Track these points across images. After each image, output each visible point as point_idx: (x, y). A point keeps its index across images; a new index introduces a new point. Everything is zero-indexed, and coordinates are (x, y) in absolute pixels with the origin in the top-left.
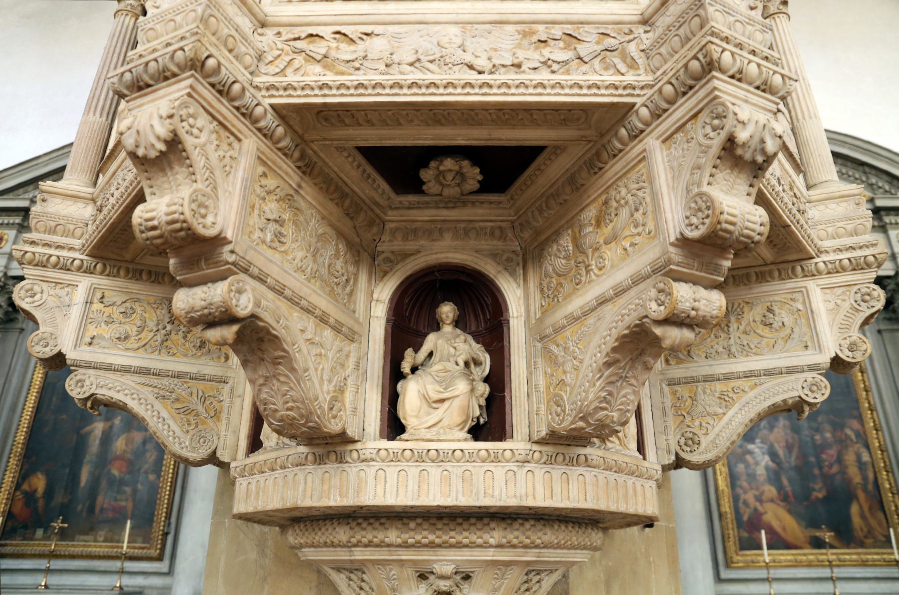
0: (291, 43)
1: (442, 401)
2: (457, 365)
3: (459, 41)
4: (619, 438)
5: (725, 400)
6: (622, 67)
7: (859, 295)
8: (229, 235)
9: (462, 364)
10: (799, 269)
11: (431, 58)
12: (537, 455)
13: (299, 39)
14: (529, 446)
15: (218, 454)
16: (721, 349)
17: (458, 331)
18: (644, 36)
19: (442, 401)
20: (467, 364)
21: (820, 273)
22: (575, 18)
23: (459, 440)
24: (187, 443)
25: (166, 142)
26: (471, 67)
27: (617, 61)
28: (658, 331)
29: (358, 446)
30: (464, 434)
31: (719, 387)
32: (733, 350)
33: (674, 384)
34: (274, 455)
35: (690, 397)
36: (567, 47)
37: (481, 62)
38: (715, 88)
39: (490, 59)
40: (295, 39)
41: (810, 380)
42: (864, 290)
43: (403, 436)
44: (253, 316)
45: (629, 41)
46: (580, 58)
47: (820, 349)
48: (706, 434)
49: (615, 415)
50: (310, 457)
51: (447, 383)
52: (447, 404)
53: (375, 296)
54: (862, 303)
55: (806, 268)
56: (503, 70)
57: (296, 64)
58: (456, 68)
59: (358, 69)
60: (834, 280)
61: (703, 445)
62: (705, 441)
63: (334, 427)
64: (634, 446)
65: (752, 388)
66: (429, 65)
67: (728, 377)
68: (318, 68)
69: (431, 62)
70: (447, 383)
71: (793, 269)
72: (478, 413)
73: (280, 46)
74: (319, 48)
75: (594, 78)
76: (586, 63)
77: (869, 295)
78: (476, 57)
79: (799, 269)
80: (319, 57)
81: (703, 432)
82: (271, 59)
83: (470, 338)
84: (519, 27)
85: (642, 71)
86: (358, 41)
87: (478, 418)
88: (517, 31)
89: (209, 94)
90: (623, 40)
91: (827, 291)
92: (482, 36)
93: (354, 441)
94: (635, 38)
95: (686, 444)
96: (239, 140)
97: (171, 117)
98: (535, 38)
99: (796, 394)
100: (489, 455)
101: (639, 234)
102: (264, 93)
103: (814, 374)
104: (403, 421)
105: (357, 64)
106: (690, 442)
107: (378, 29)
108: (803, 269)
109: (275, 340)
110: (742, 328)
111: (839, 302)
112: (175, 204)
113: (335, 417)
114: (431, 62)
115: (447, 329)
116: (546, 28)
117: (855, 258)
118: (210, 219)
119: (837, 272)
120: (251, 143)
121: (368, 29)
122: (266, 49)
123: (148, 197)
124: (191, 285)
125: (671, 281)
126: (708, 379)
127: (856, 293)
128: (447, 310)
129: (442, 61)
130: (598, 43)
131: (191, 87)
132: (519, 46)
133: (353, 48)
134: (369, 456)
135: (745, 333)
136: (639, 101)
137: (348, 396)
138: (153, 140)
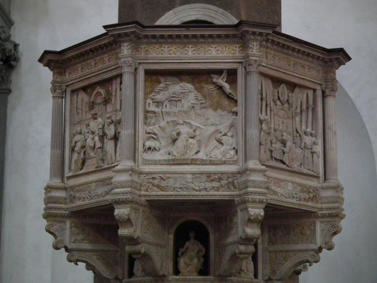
0: (148, 180)
1: (190, 264)
2: (195, 253)
3: (191, 180)
4: (245, 273)
5: (285, 259)
6: (232, 188)
7: (331, 225)
8: (140, 236)
9: (196, 253)
10: (313, 215)
11: (184, 186)
12: (216, 280)
13: (150, 178)
14: (214, 277)
15: (119, 276)
16: (286, 241)
17: (195, 241)
18: (239, 178)
19: (190, 264)
20: (198, 252)
21: (319, 217)
22: (221, 172)
23: (195, 276)
24: (108, 274)
25: (127, 219)
26: (194, 190)
27: (231, 186)
28: (238, 255)
29: (167, 277)
30: (196, 274)
31: (284, 254)
32: (290, 242)
33: (270, 252)
34: (141, 279)
35: (275, 257)
36: (219, 181)
37: (197, 188)
38: (247, 206)
39: (199, 187)
40: (149, 179)
41: (311, 254)
42: (333, 224)
43: (180, 275)
44: (145, 252)
45: (235, 179)
46: (221, 185)
47: (315, 243)
48: (278, 270)
49: (234, 271)
50: (153, 280)
51: (191, 259)
52: (191, 266)
53: (170, 232)
54: (332, 228)
55: (315, 215)
56: (203, 190)
57: (150, 187)
58: (191, 190)
59: (166, 189)
60: (324, 220)
61: (277, 274)
62: (278, 273)
63: (162, 273)
64: (252, 275)
65: (294, 255)
66: (184, 189)
67: (287, 251)
68: (156, 189)
69: (184, 188)
70: (191, 259)
71: (311, 215)
72: (200, 267)
73: (146, 181)
74: (156, 182)
75: (224, 193)
76: (223, 187)
77: (334, 225)
78: (196, 186)
79: (313, 215)
80: (156, 185)
81: (278, 269)
82: (144, 185)
83: (198, 243)
84: (207, 175)
85: (237, 190)
86: (166, 180)
87: (201, 269)
88: (206, 176)
89: (134, 206)
90: (234, 179)
91: (322, 223)
92: (197, 178)
93: (166, 276)
94: (237, 178)
95: (272, 273)
96: (139, 210)
97: (128, 215)
98: (211, 179)
99: (306, 258)
100: (203, 279)
101: (236, 230)
102: (143, 197)
103: (313, 252)
104: (180, 270)
105: (166, 188)
106: (273, 273)
107: (171, 176)
108: (314, 215)
109: (148, 255)
110: (294, 234)
111: (325, 227)
112: (129, 232)
113: (161, 270)
114: (184, 188)
115: (192, 240)
116: (214, 175)
117: (330, 213)
118: (136, 234)
119: (325, 217)
120: (141, 209)
121: (168, 175)
122: (142, 182)
123: (120, 227)
124: (129, 245)
125: (240, 245)
126: (281, 251)
127: (330, 225)
128: (192, 235)
129: (187, 188)
130: (227, 180)
131: (131, 206)
132: (206, 181)
133: (164, 181)
134: (170, 280)
135: (294, 236)
136: (236, 199)
137: (164, 264)
138: (123, 219)
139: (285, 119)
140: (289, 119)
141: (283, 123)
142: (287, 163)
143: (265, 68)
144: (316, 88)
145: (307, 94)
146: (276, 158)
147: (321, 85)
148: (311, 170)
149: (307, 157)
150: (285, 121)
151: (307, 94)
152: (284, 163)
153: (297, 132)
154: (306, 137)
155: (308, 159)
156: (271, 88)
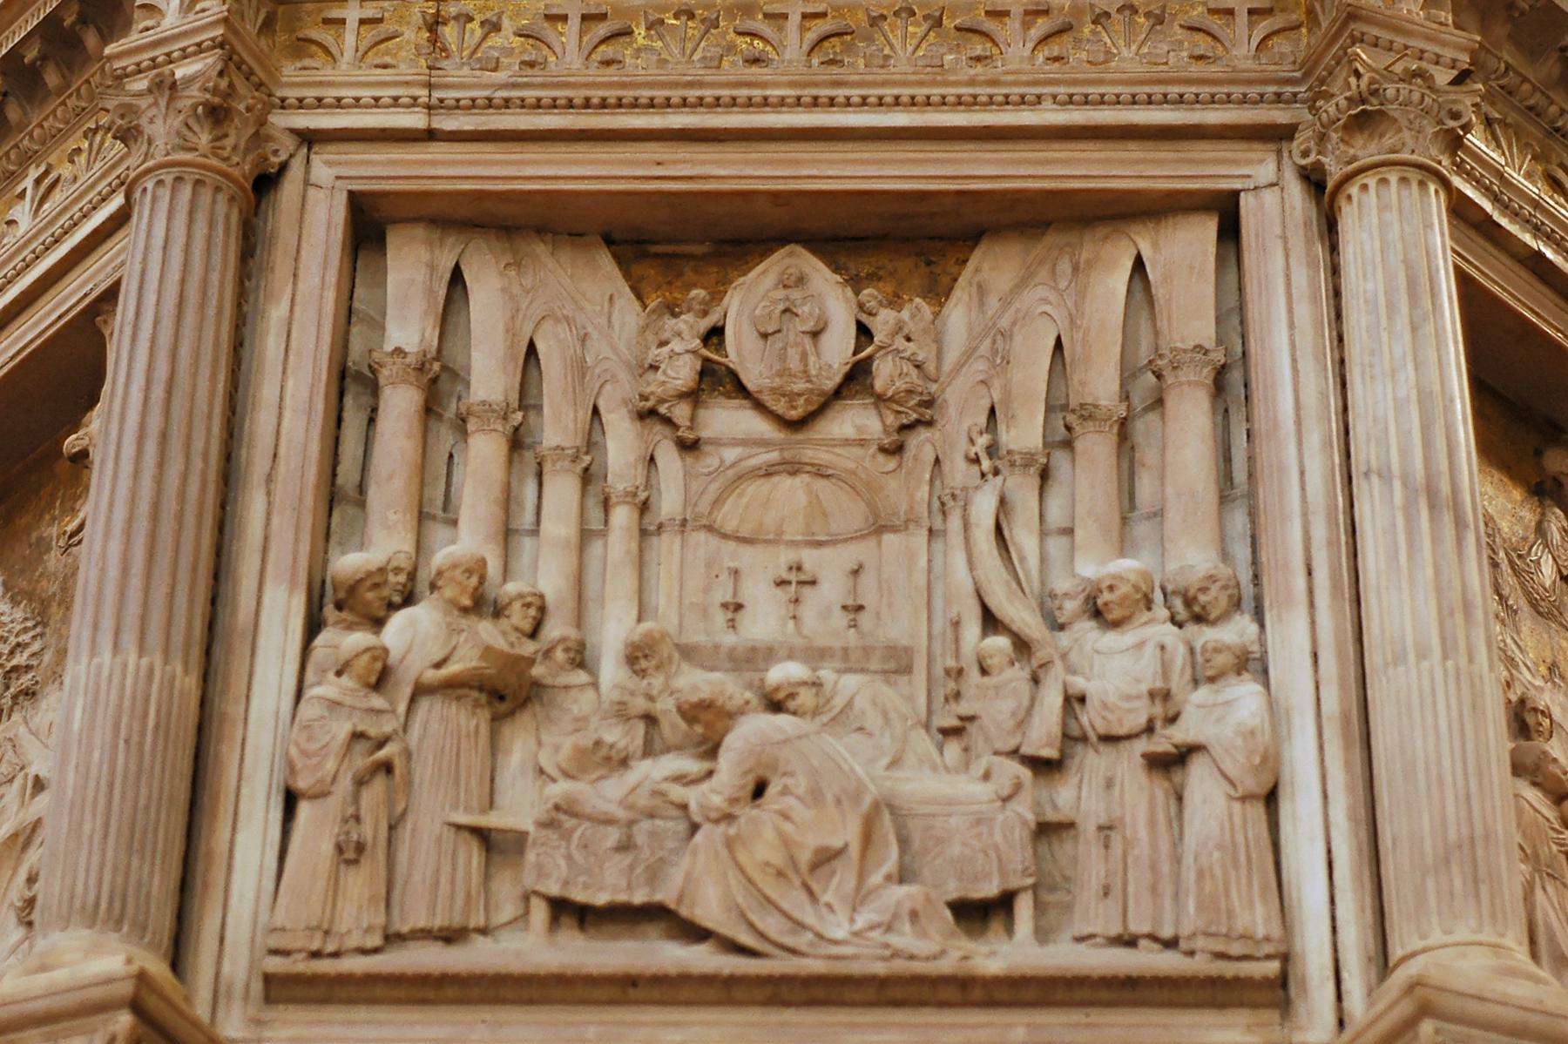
139: (820, 544)
140: (889, 538)
141: (795, 582)
142: (708, 910)
143: (436, 151)
144: (1237, 185)
145: (1139, 265)
146: (579, 896)
147: (1278, 135)
148: (1153, 938)
149: (1100, 828)
150: (830, 566)
151: (1139, 265)
152: (696, 933)
153: (991, 621)
154: (1111, 639)
155: (1116, 837)
156: (628, 314)
